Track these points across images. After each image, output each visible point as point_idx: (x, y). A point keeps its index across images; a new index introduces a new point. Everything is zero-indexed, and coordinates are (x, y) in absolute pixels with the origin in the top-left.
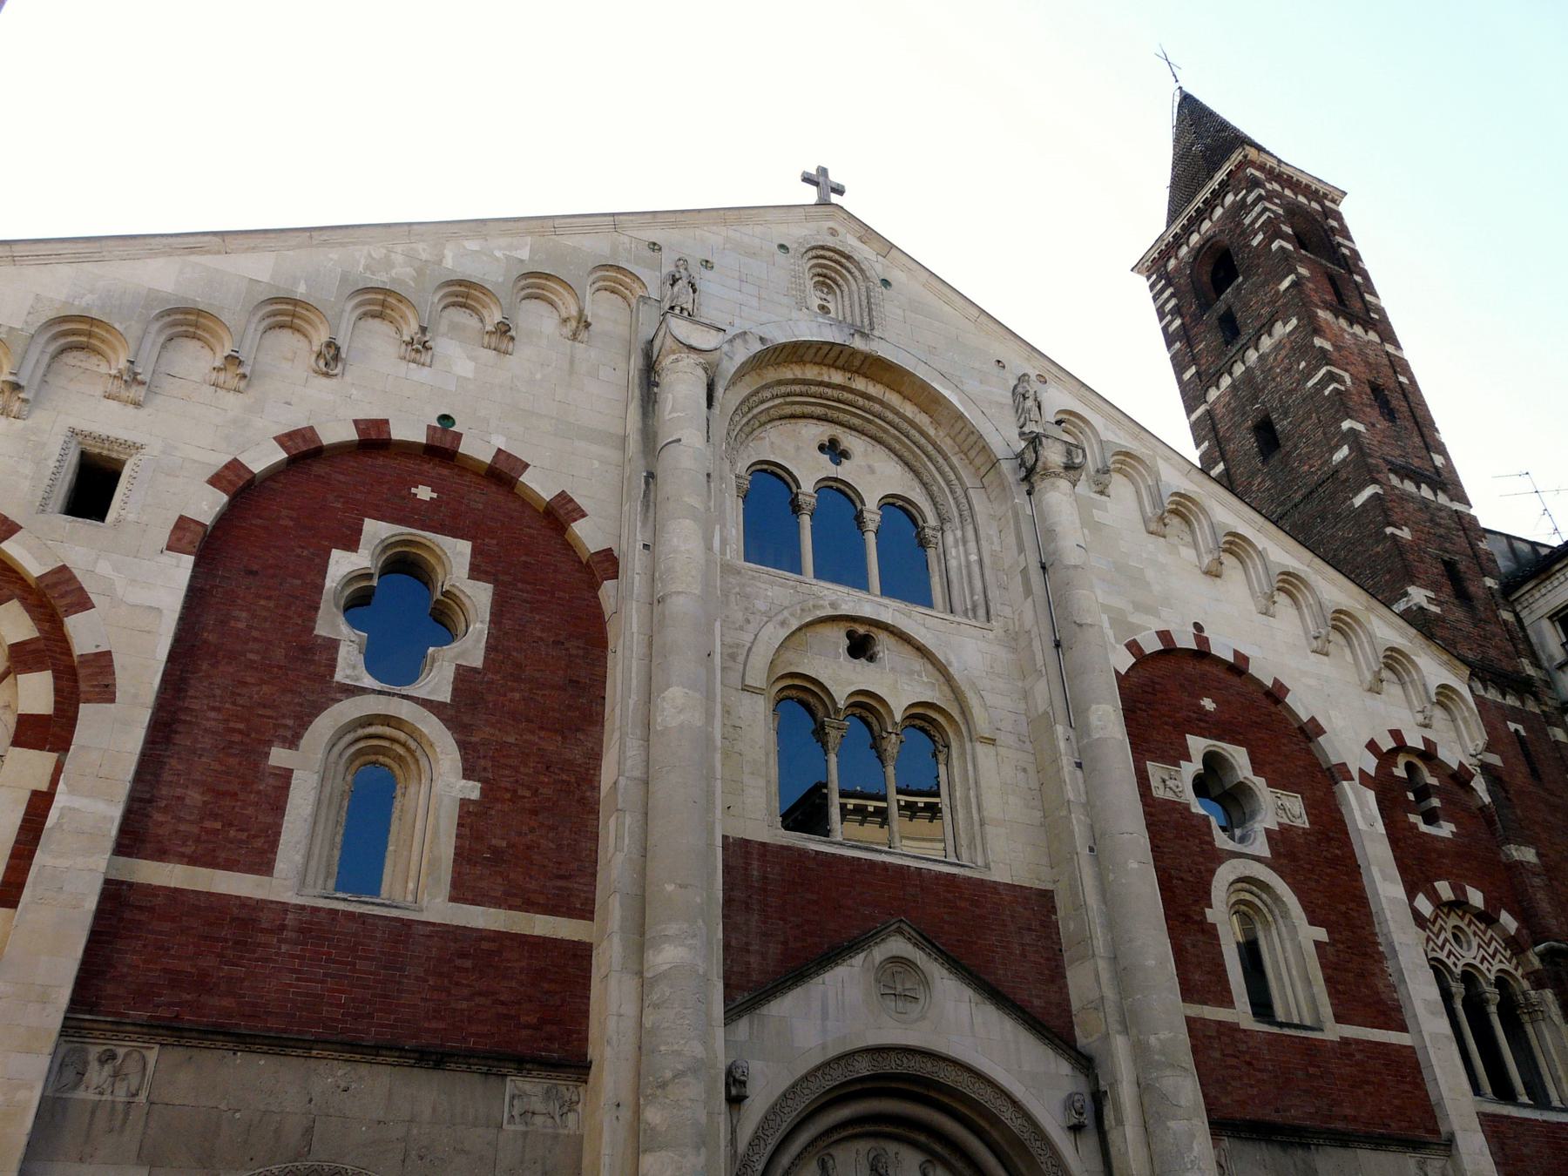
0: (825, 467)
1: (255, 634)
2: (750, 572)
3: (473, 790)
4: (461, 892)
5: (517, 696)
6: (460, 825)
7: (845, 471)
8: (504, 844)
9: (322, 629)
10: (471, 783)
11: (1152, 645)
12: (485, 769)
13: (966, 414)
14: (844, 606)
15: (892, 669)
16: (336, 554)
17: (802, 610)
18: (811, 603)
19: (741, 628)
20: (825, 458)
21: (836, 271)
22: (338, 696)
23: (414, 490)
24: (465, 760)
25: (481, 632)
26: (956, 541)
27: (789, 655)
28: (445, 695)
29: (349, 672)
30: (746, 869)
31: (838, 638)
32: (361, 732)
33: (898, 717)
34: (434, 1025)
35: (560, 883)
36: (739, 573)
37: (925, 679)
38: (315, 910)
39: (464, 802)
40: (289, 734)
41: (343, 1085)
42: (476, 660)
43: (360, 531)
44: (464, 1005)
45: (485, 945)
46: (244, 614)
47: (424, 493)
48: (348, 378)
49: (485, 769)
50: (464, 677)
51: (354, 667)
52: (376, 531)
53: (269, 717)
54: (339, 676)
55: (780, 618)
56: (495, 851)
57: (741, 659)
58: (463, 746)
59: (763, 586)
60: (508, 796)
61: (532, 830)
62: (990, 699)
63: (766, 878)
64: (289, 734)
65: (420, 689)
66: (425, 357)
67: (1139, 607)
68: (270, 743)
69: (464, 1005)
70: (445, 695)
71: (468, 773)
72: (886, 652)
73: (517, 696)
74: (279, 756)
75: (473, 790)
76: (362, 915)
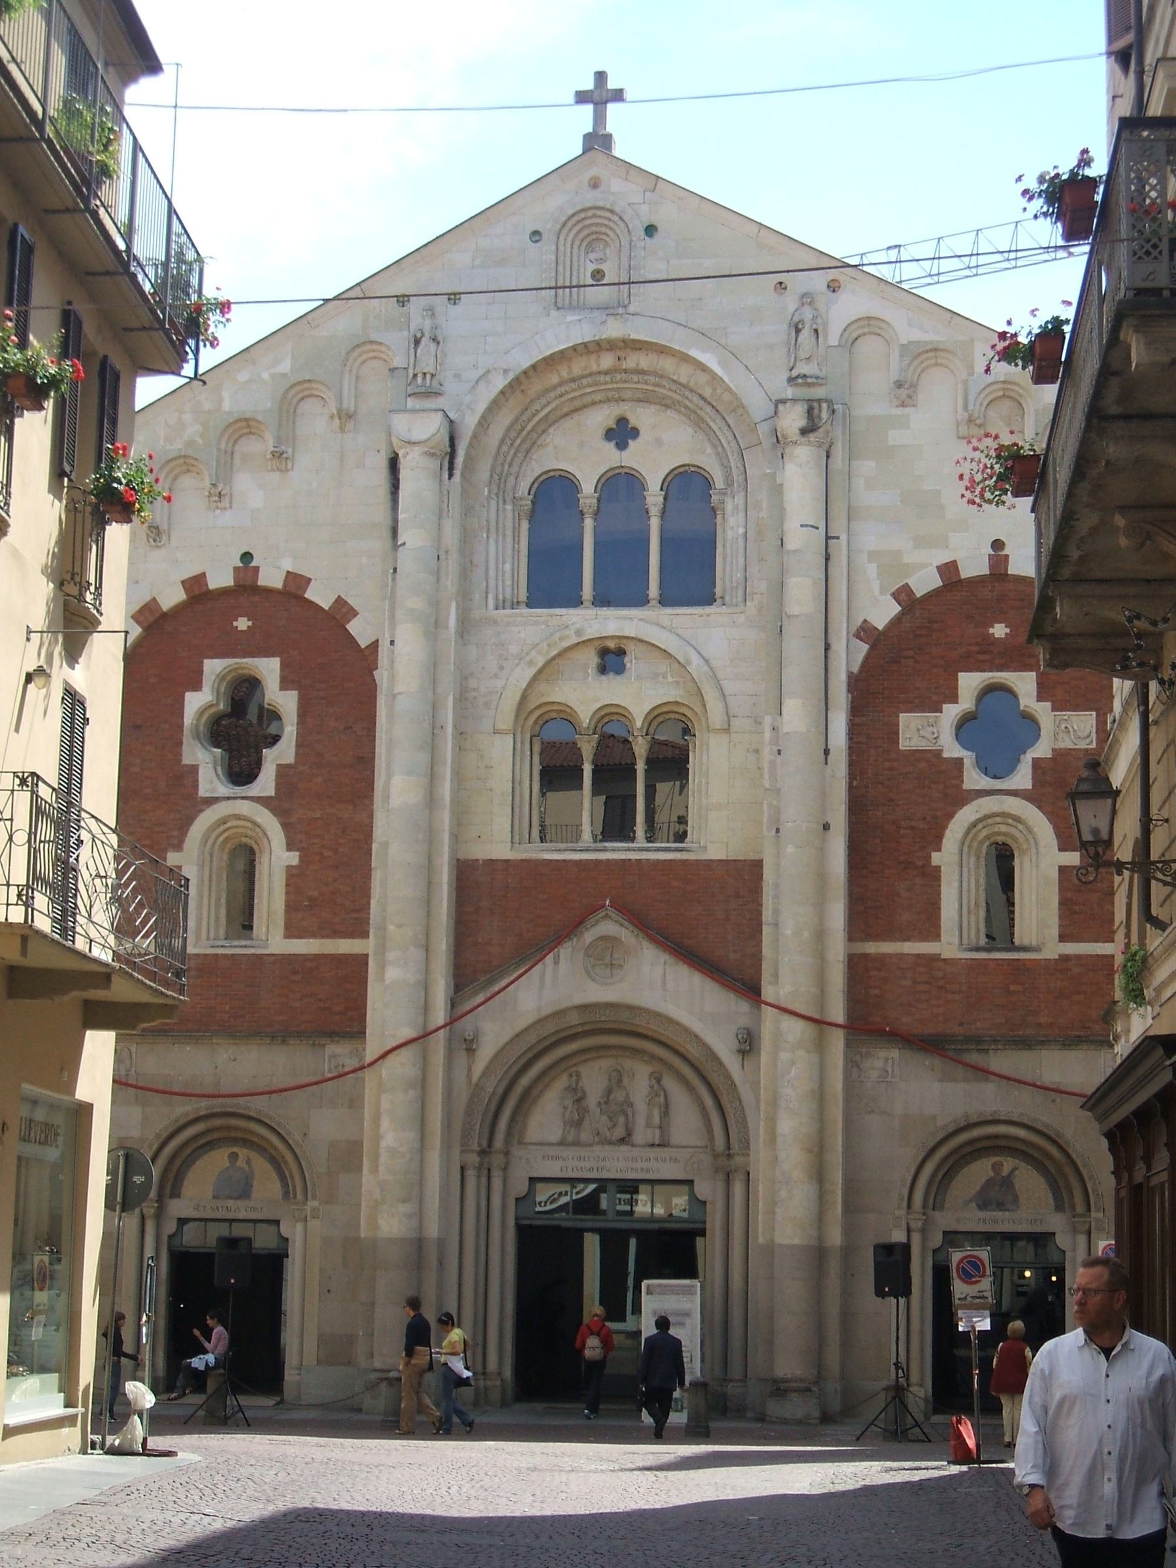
0: (611, 457)
1: (147, 773)
2: (506, 619)
3: (293, 858)
4: (291, 932)
5: (320, 779)
6: (287, 885)
7: (633, 457)
8: (316, 894)
9: (187, 760)
10: (292, 854)
11: (925, 582)
12: (301, 841)
13: (726, 379)
14: (589, 631)
15: (638, 677)
16: (189, 696)
17: (549, 645)
18: (557, 636)
19: (495, 676)
20: (633, 422)
21: (611, 229)
22: (203, 807)
23: (235, 624)
24: (287, 837)
25: (292, 732)
26: (736, 508)
27: (542, 687)
28: (270, 791)
29: (208, 786)
31: (591, 659)
32: (222, 828)
33: (639, 724)
34: (280, 1018)
35: (356, 915)
36: (496, 622)
37: (670, 679)
38: (206, 955)
39: (289, 868)
40: (176, 842)
41: (232, 1057)
42: (289, 758)
43: (200, 672)
44: (297, 1004)
45: (308, 964)
46: (138, 761)
47: (243, 624)
48: (174, 542)
49: (301, 841)
50: (283, 772)
51: (211, 782)
52: (213, 667)
53: (163, 832)
54: (203, 792)
55: (528, 658)
56: (310, 899)
57: (493, 706)
58: (285, 826)
59: (516, 629)
60: (317, 858)
61: (335, 880)
62: (729, 687)
64: (176, 842)
65: (255, 789)
66: (225, 502)
67: (920, 542)
68: (165, 851)
69: (297, 1004)
70: (270, 791)
71: (290, 848)
72: (634, 661)
73: (320, 779)
74: (172, 859)
75: (293, 858)
76: (233, 955)
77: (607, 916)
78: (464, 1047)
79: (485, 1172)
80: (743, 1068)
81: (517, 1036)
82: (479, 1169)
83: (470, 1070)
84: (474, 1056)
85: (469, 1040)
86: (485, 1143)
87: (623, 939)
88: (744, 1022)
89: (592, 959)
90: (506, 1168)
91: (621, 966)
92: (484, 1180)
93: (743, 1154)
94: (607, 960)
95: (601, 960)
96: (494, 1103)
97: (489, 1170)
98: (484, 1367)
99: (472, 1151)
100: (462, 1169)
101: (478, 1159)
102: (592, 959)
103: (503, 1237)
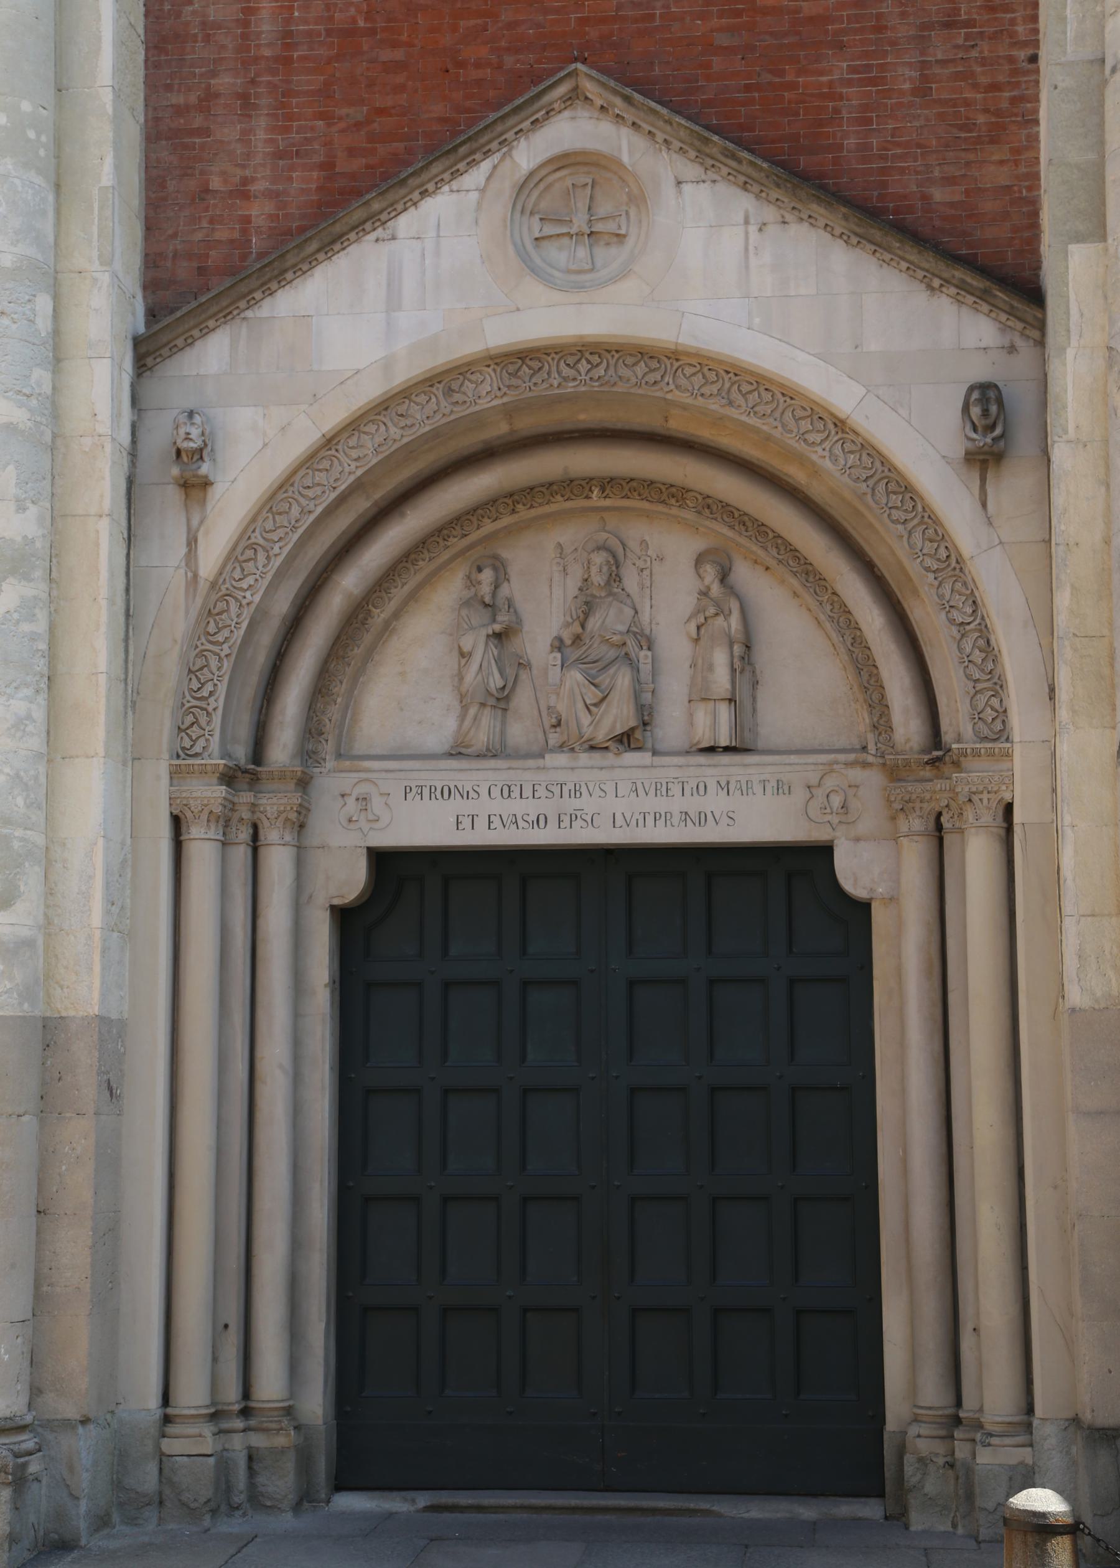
30: (246, 24)
63: (288, 34)
77: (575, 97)
78: (175, 471)
79: (245, 834)
80: (984, 505)
81: (330, 442)
82: (225, 820)
83: (192, 542)
84: (203, 502)
85: (193, 452)
86: (241, 753)
87: (625, 159)
88: (980, 371)
89: (535, 220)
90: (302, 826)
91: (620, 237)
92: (240, 855)
93: (991, 754)
94: (580, 222)
95: (559, 221)
96: (267, 638)
97: (255, 827)
98: (246, 1394)
99: (203, 771)
100: (177, 822)
101: (221, 791)
102: (535, 220)
103: (297, 1015)
